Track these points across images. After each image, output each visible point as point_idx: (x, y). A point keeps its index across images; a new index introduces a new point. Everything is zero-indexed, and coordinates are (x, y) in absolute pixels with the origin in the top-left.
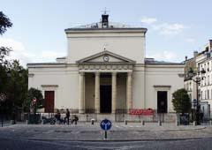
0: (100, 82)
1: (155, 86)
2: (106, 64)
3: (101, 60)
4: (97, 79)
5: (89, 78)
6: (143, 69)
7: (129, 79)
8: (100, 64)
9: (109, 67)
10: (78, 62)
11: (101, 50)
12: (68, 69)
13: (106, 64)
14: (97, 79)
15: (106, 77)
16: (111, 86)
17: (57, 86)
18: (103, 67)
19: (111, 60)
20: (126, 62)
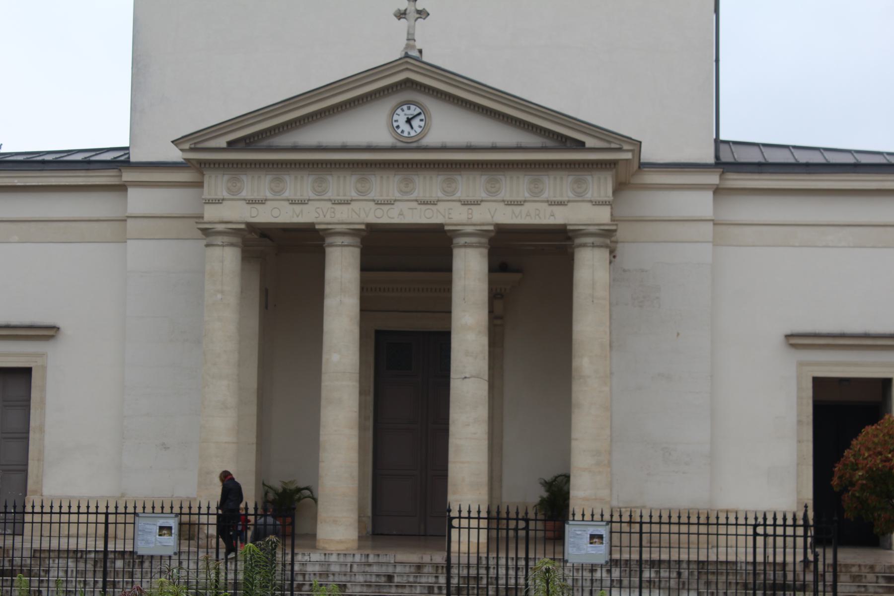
0: (367, 308)
1: (797, 341)
2: (407, 162)
3: (370, 129)
4: (342, 271)
5: (282, 262)
6: (702, 204)
7: (590, 269)
8: (365, 164)
9: (428, 186)
10: (191, 141)
11: (379, 46)
12: (140, 201)
13: (407, 162)
14: (342, 271)
15: (406, 260)
16: (440, 343)
17: (47, 333)
18: (385, 186)
19: (449, 129)
20: (562, 145)
